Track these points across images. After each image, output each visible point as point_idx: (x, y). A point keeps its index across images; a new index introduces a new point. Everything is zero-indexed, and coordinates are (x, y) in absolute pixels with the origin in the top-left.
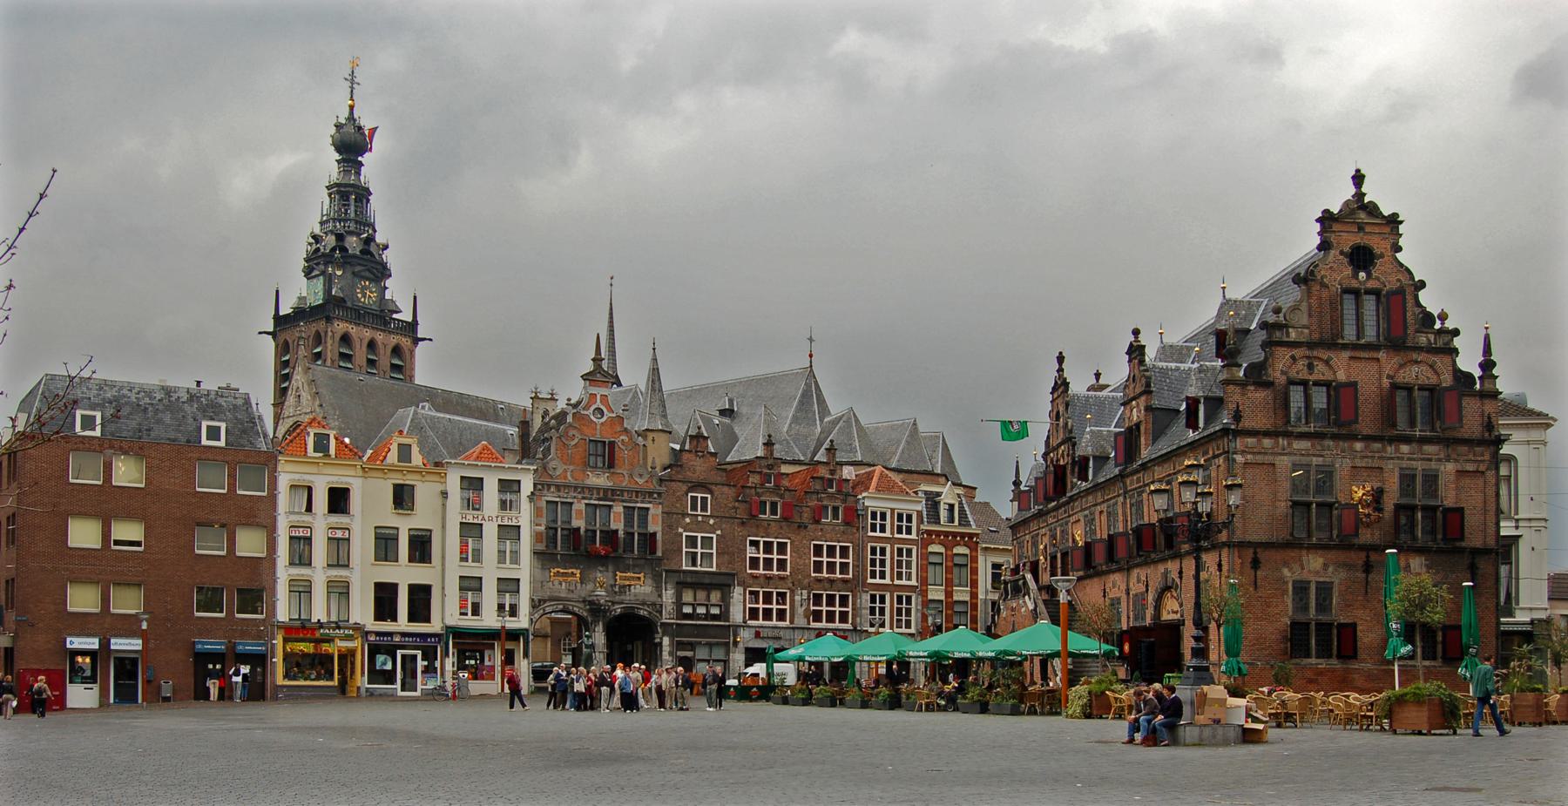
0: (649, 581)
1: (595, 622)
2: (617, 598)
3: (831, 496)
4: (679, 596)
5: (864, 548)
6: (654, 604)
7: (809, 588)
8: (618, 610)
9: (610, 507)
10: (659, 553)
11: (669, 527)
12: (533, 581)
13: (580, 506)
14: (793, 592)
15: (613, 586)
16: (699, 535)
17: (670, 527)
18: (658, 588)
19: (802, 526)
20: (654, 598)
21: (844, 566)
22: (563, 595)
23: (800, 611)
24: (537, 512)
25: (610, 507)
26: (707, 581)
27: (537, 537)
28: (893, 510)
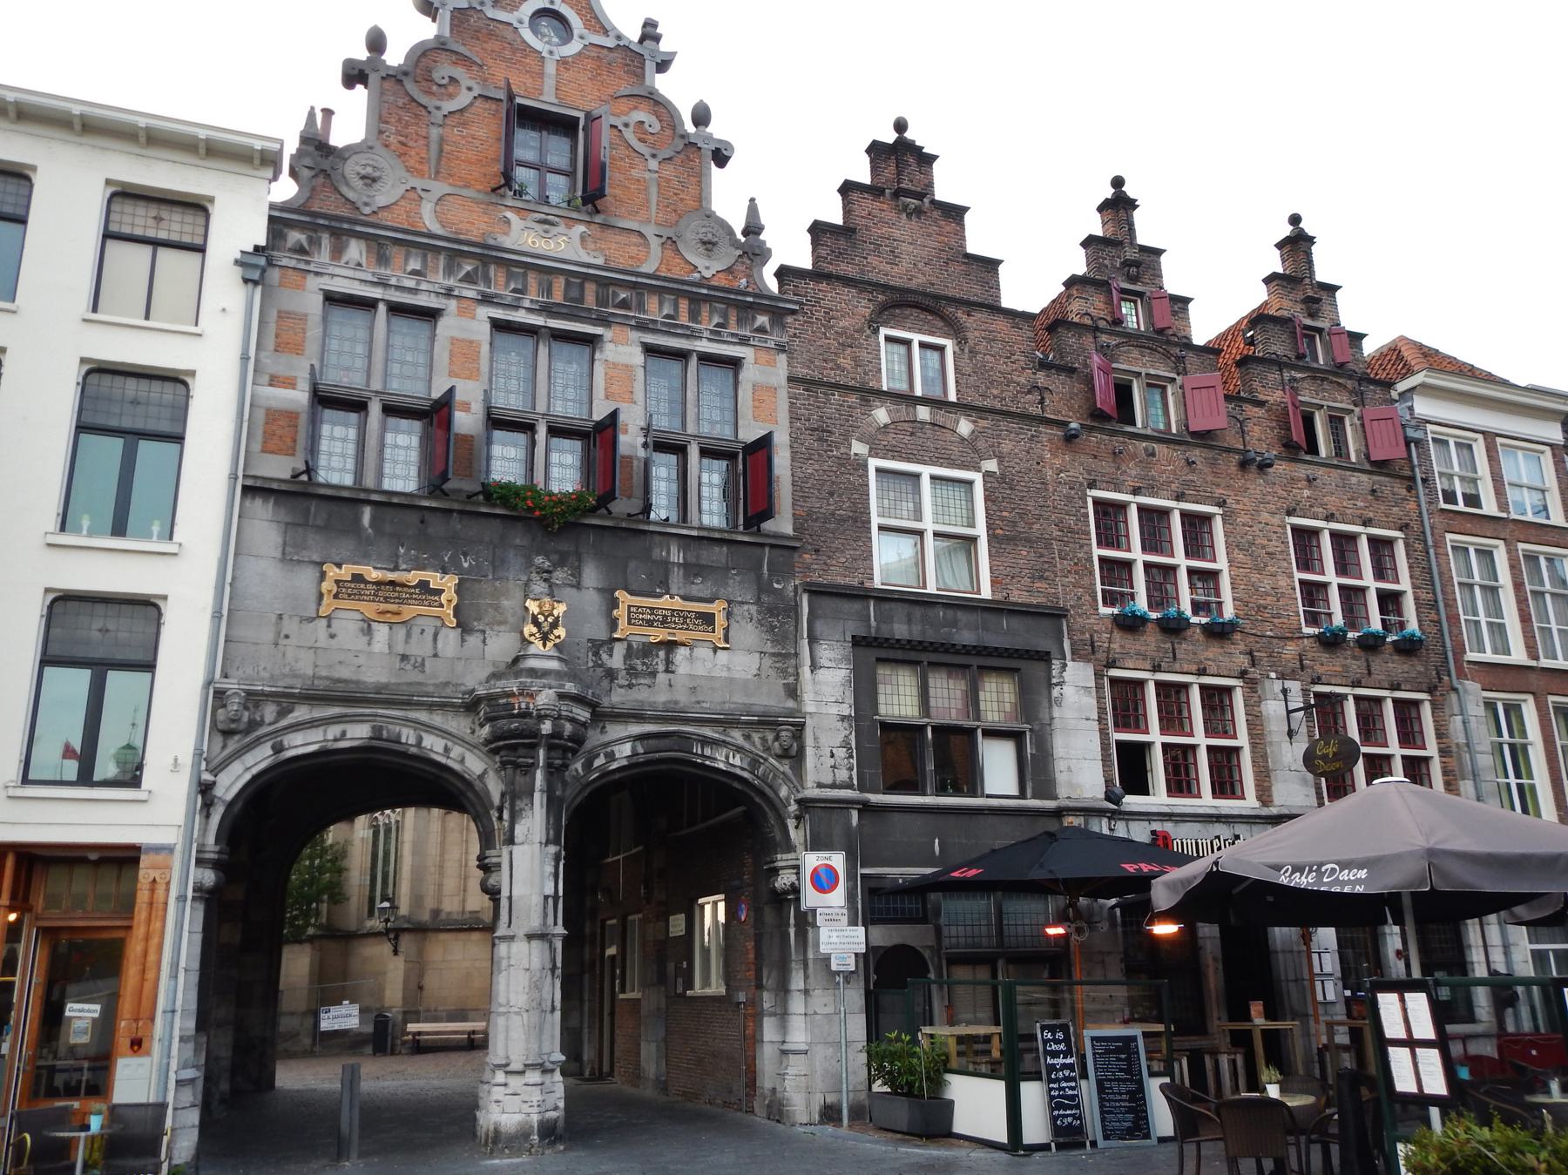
0: (748, 633)
1: (516, 796)
2: (618, 697)
3: (1318, 376)
4: (864, 691)
5: (1439, 543)
6: (767, 722)
7: (1299, 669)
8: (620, 746)
9: (591, 341)
10: (782, 524)
11: (818, 436)
12: (231, 612)
13: (466, 325)
14: (1252, 685)
15: (596, 646)
16: (926, 471)
17: (821, 432)
18: (784, 659)
19: (1251, 464)
20: (770, 699)
21: (1390, 601)
22: (375, 673)
23: (1290, 754)
24: (273, 335)
25: (591, 341)
26: (966, 637)
27: (266, 428)
28: (1490, 436)
